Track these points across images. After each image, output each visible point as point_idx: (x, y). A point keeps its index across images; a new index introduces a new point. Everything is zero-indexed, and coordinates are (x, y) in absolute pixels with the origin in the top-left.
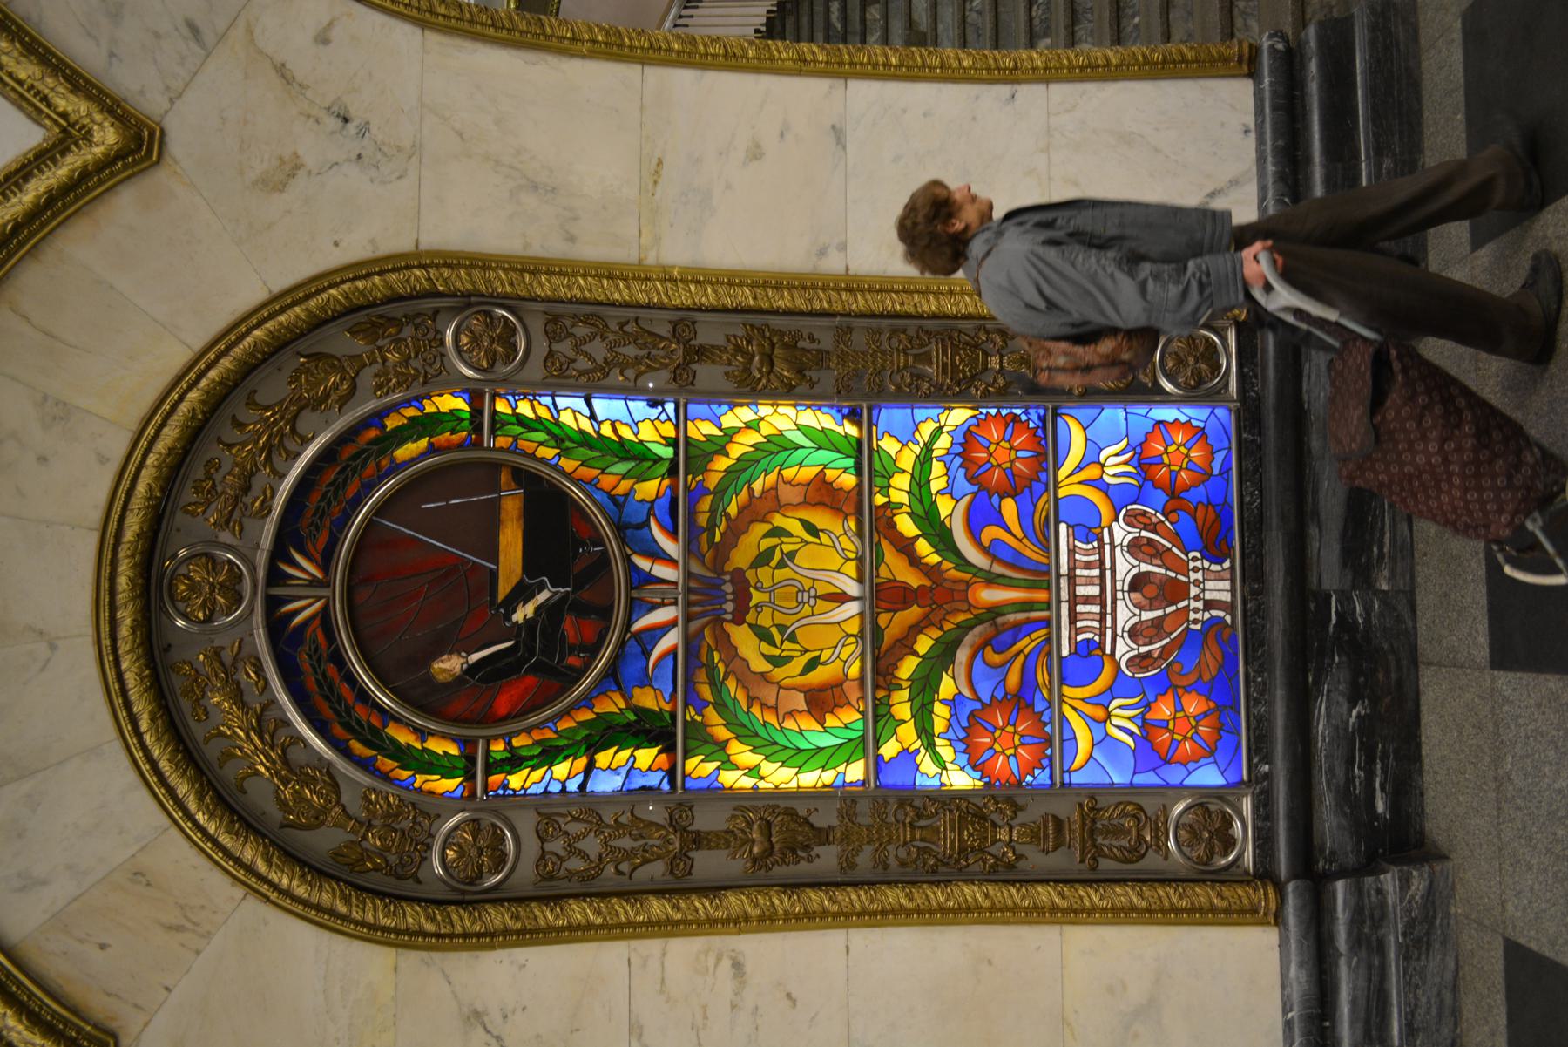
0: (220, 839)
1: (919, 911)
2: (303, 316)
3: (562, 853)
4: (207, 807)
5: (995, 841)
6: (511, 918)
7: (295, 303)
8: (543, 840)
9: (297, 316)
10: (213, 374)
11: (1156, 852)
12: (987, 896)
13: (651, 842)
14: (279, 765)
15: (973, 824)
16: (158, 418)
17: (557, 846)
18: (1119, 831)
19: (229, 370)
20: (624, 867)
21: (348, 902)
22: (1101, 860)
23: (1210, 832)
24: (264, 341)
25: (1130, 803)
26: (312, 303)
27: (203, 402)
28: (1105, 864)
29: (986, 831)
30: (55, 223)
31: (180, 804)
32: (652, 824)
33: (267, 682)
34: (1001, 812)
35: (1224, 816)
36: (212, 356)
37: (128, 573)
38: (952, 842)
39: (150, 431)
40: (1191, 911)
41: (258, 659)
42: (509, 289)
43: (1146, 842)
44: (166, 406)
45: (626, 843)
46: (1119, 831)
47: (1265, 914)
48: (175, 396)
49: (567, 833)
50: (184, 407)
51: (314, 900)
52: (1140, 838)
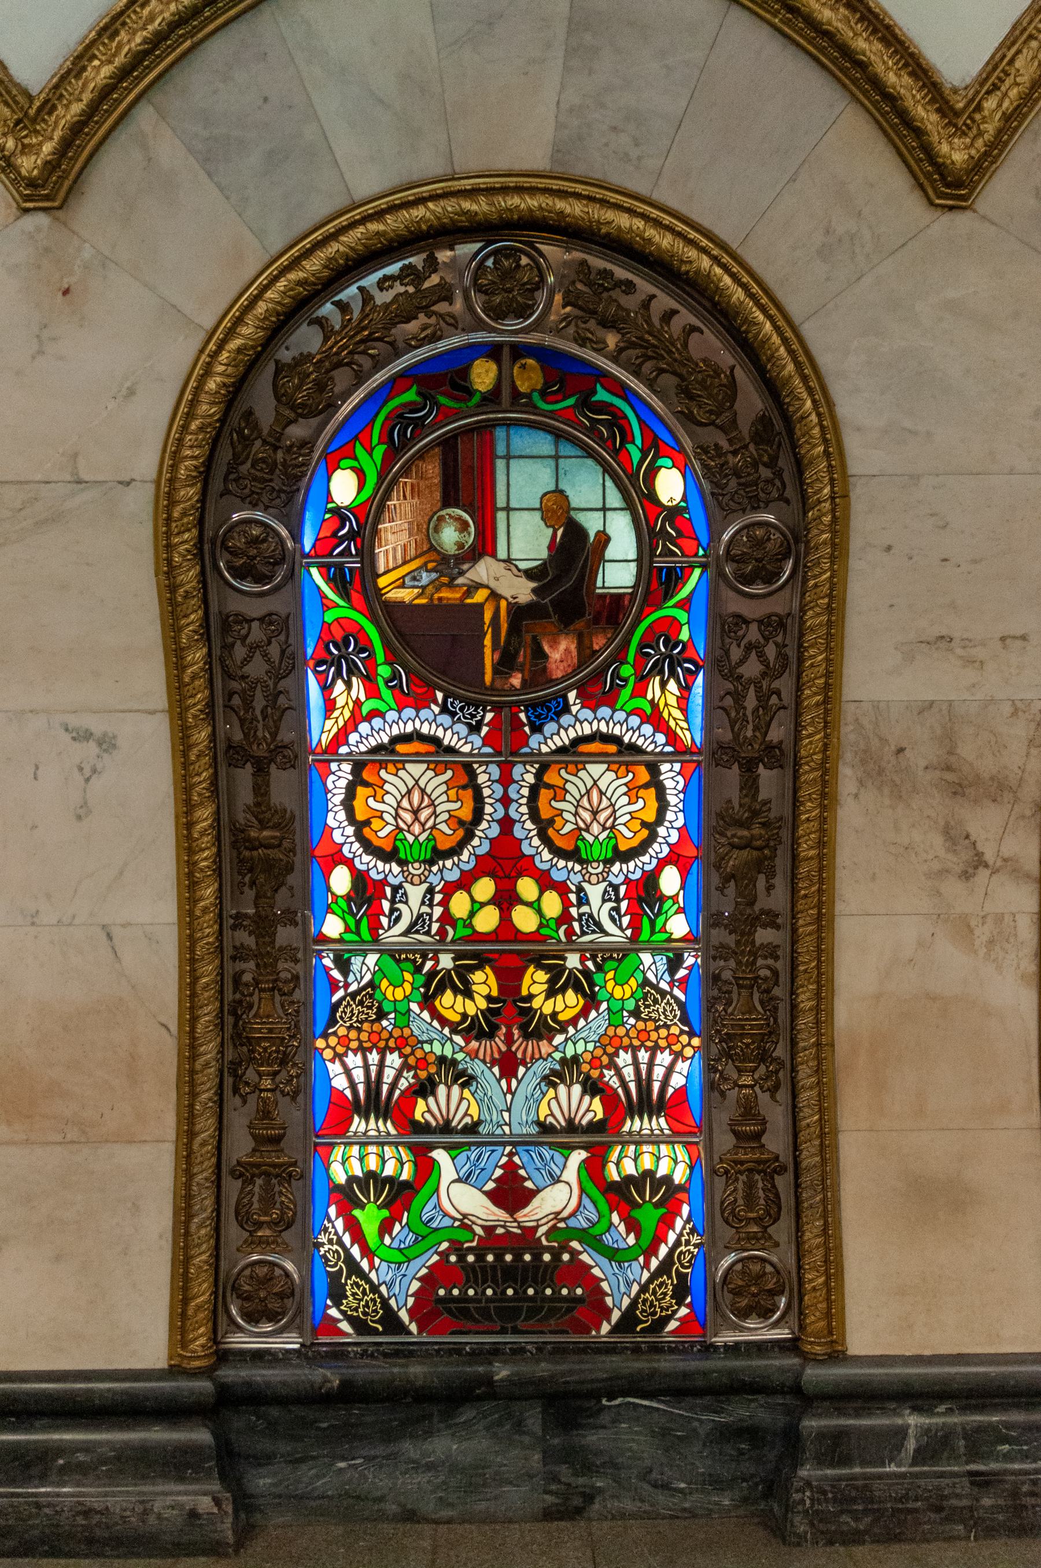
0: (261, 303)
1: (193, 995)
2: (785, 373)
3: (248, 641)
4: (292, 289)
5: (260, 1075)
6: (186, 592)
7: (798, 365)
8: (261, 620)
9: (784, 367)
10: (727, 280)
11: (245, 1242)
12: (207, 1065)
13: (260, 726)
14: (335, 359)
15: (278, 1051)
16: (681, 227)
17: (257, 633)
18: (268, 1200)
19: (730, 296)
20: (236, 701)
21: (201, 429)
22: (240, 1182)
23: (266, 1298)
24: (759, 333)
25: (295, 1214)
26: (797, 381)
27: (698, 272)
28: (232, 1188)
29: (269, 1065)
30: (877, 115)
31: (295, 264)
32: (277, 728)
33: (416, 347)
34: (289, 1082)
35: (278, 1314)
36: (746, 279)
37: (523, 206)
38: (259, 1031)
39: (667, 220)
40: (186, 1278)
41: (440, 338)
42: (811, 583)
43: (255, 1231)
44: (693, 235)
45: (259, 702)
46: (268, 1200)
47: (180, 1355)
48: (704, 242)
49: (269, 643)
50: (692, 253)
51: (203, 397)
52: (260, 1225)
